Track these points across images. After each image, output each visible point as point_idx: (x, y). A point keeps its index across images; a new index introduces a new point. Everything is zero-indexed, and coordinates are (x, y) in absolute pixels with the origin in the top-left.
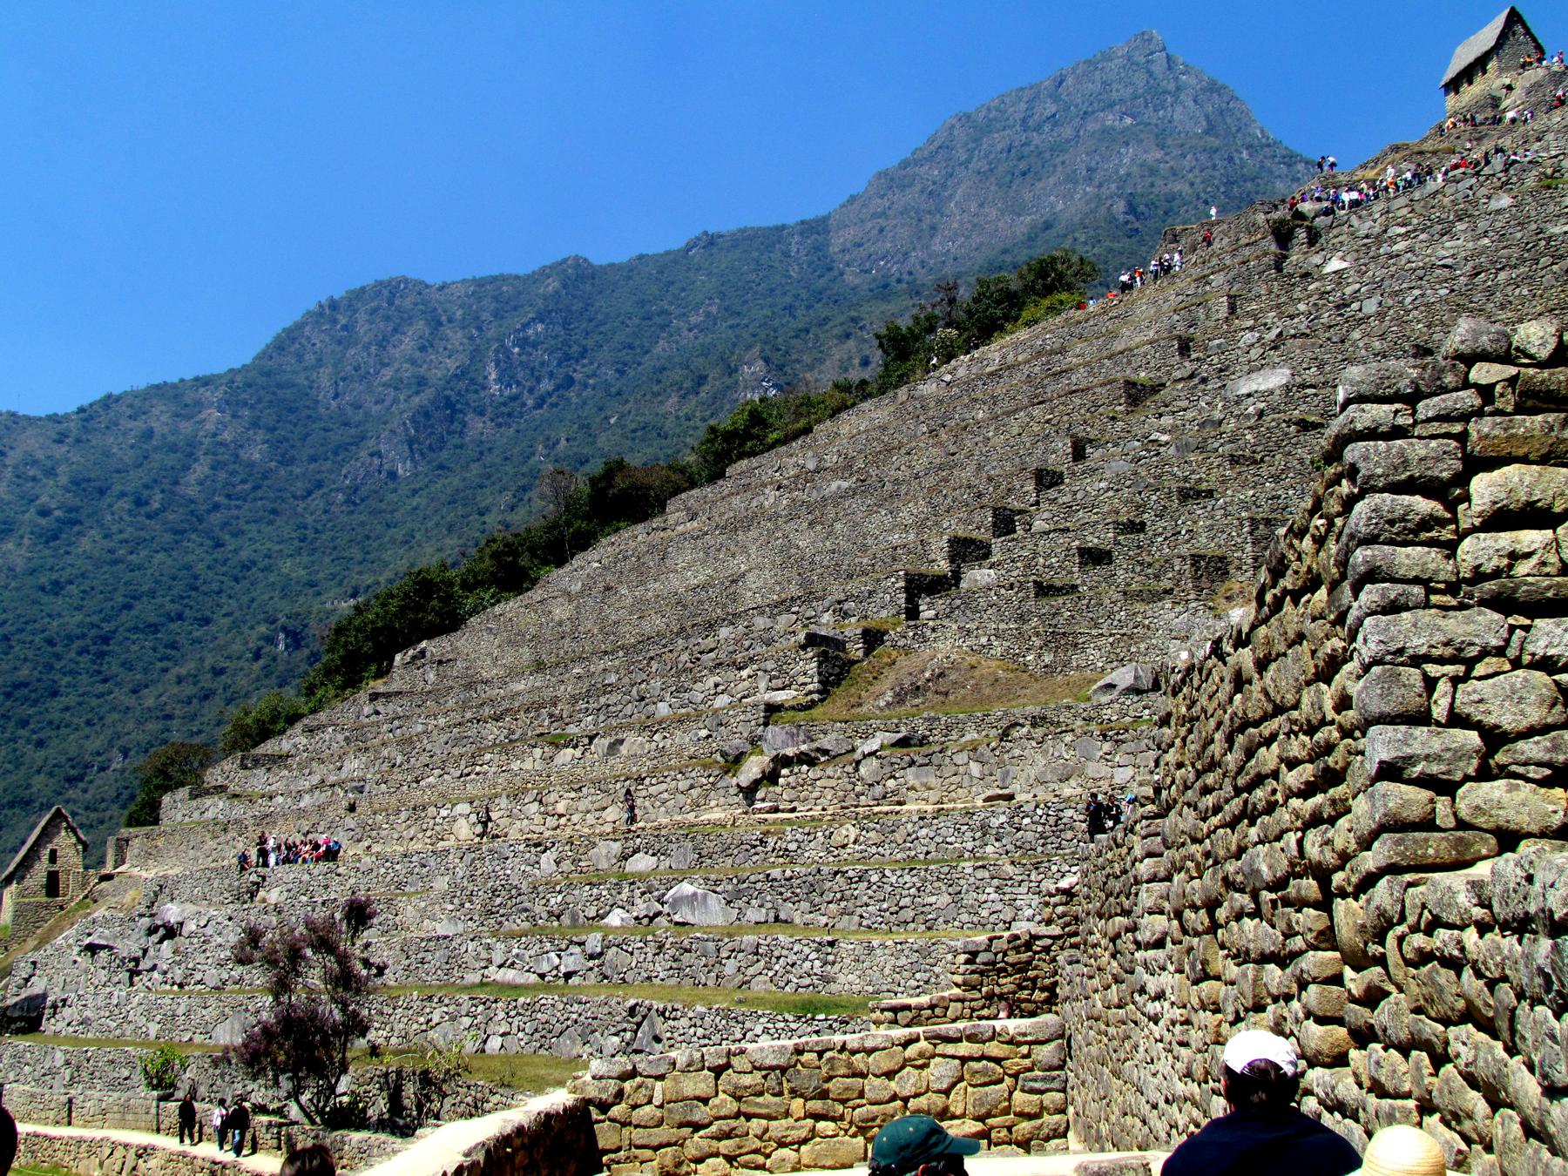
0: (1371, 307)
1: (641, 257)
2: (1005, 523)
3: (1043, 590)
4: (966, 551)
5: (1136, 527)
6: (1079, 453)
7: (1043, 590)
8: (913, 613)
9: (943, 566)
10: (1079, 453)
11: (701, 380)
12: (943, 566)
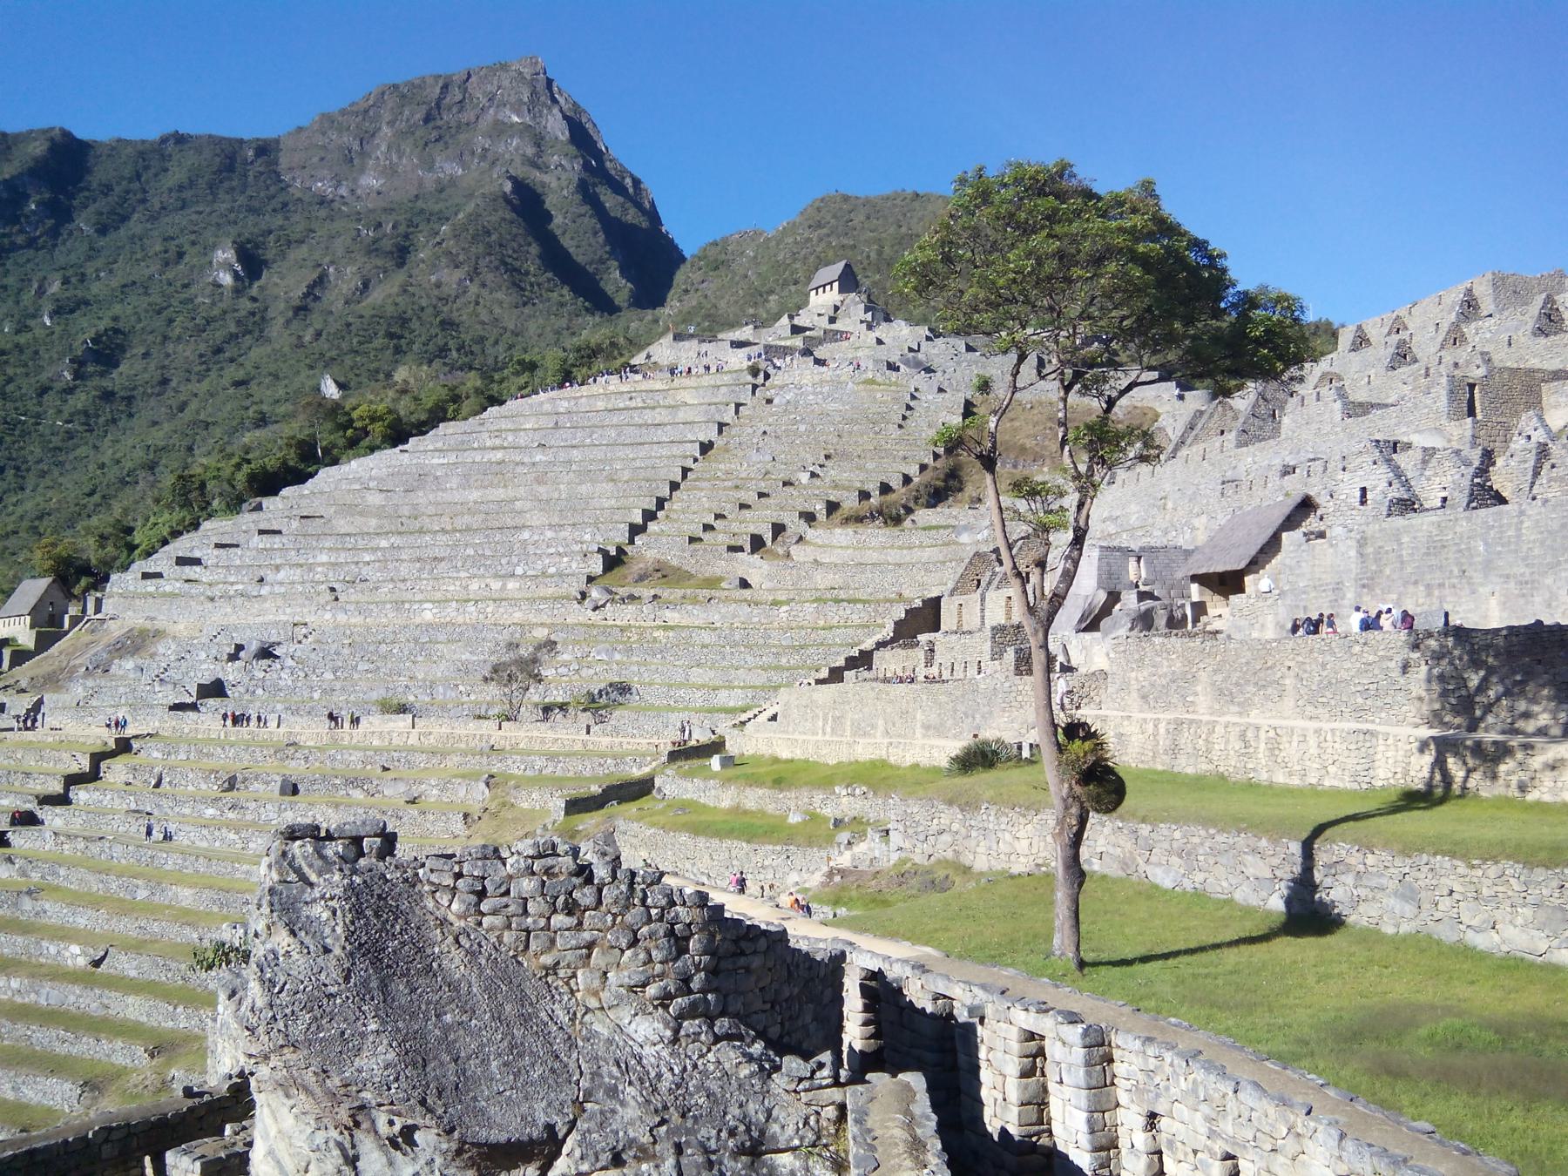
0: (802, 428)
1: (119, 140)
2: (661, 503)
3: (692, 540)
4: (649, 516)
5: (724, 517)
6: (684, 477)
7: (692, 540)
8: (632, 542)
9: (639, 520)
10: (684, 477)
11: (181, 255)
12: (639, 520)
